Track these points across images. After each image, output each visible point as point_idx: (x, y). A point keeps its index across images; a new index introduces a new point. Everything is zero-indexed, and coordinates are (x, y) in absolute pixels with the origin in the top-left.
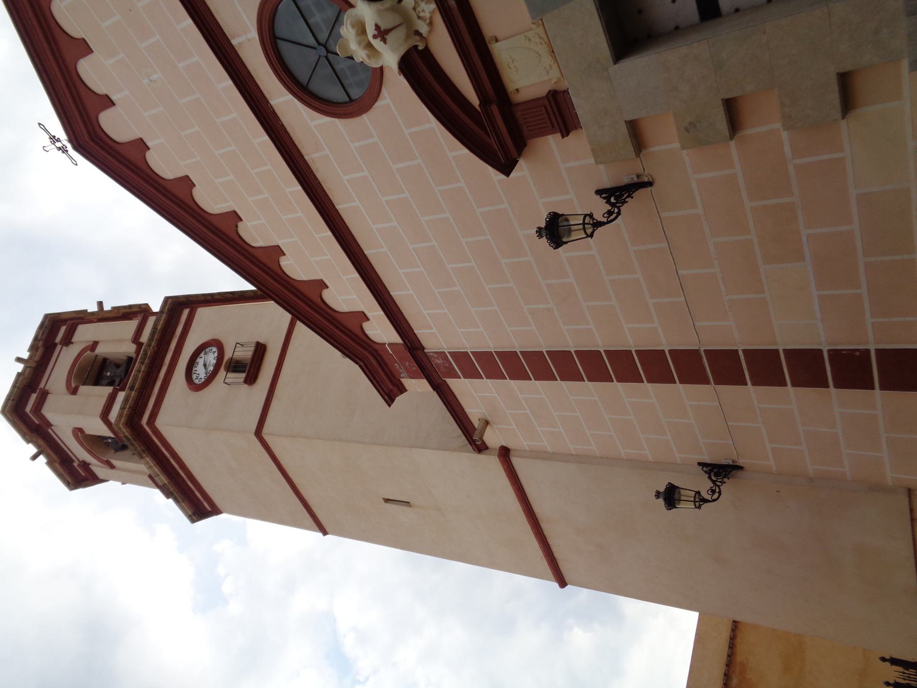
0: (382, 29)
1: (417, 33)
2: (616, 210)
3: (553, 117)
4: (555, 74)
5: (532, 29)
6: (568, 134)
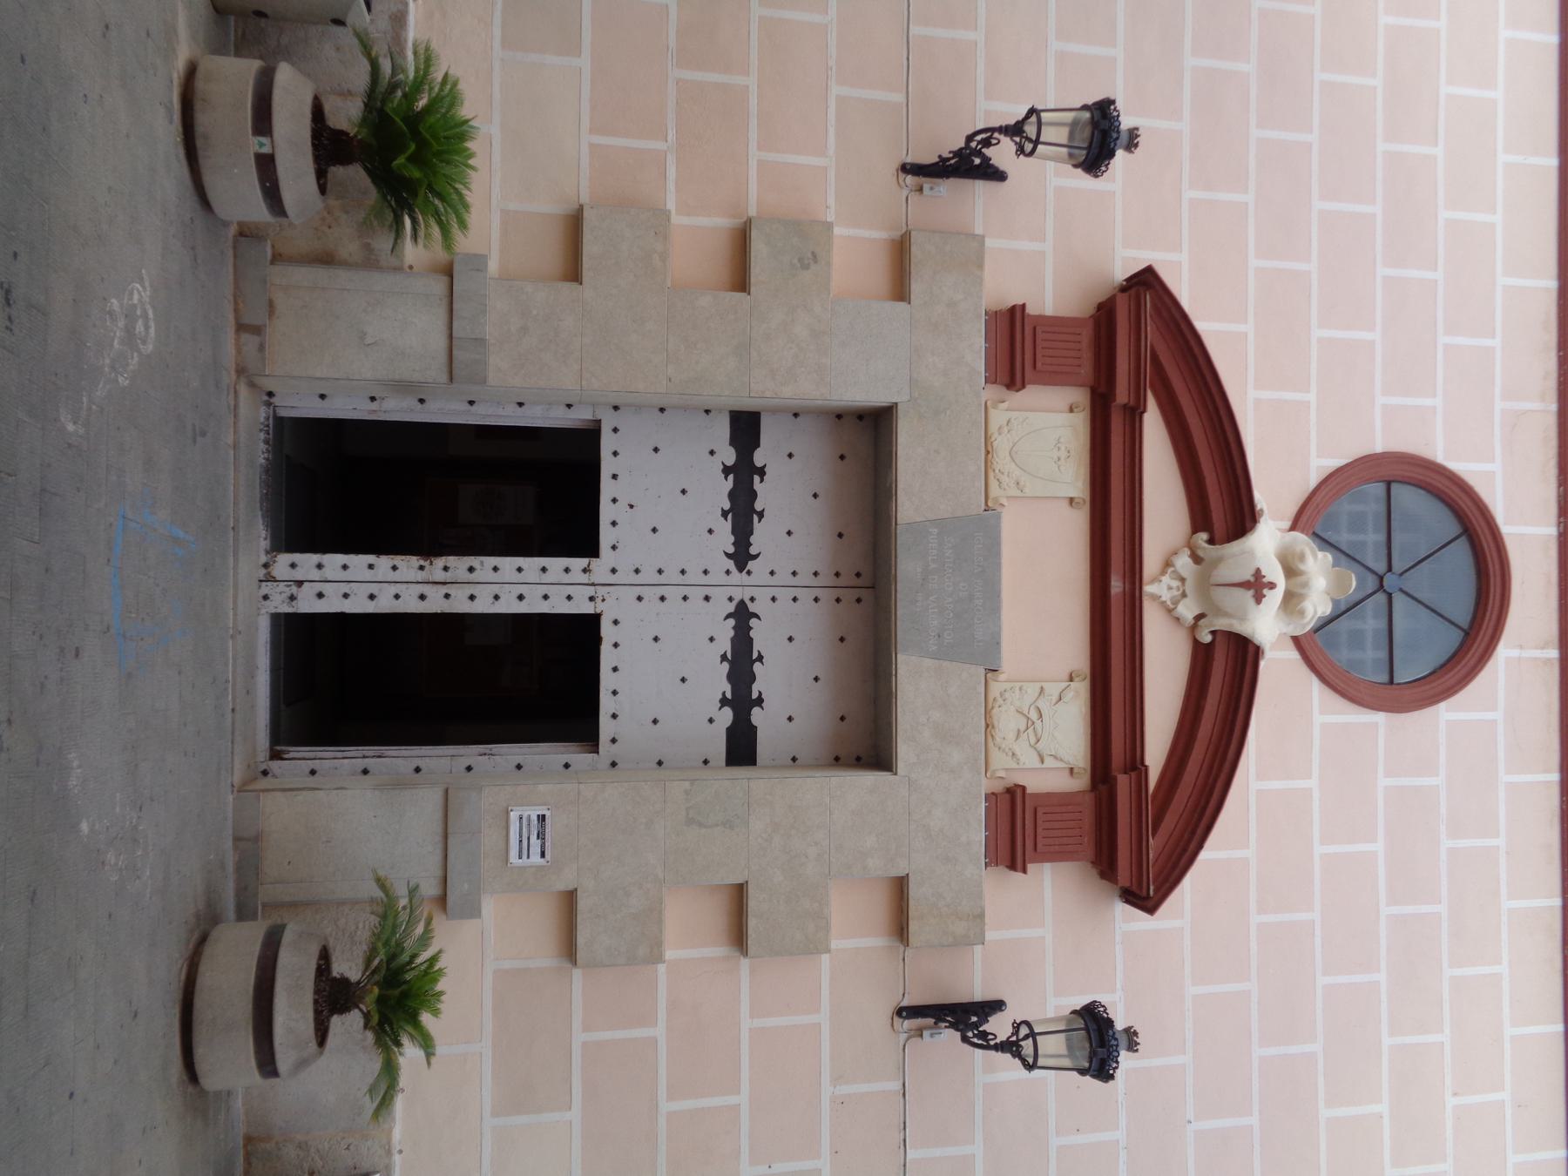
0: (1251, 592)
1: (1197, 559)
2: (973, 144)
3: (1028, 356)
4: (998, 417)
5: (1008, 497)
6: (1014, 307)
